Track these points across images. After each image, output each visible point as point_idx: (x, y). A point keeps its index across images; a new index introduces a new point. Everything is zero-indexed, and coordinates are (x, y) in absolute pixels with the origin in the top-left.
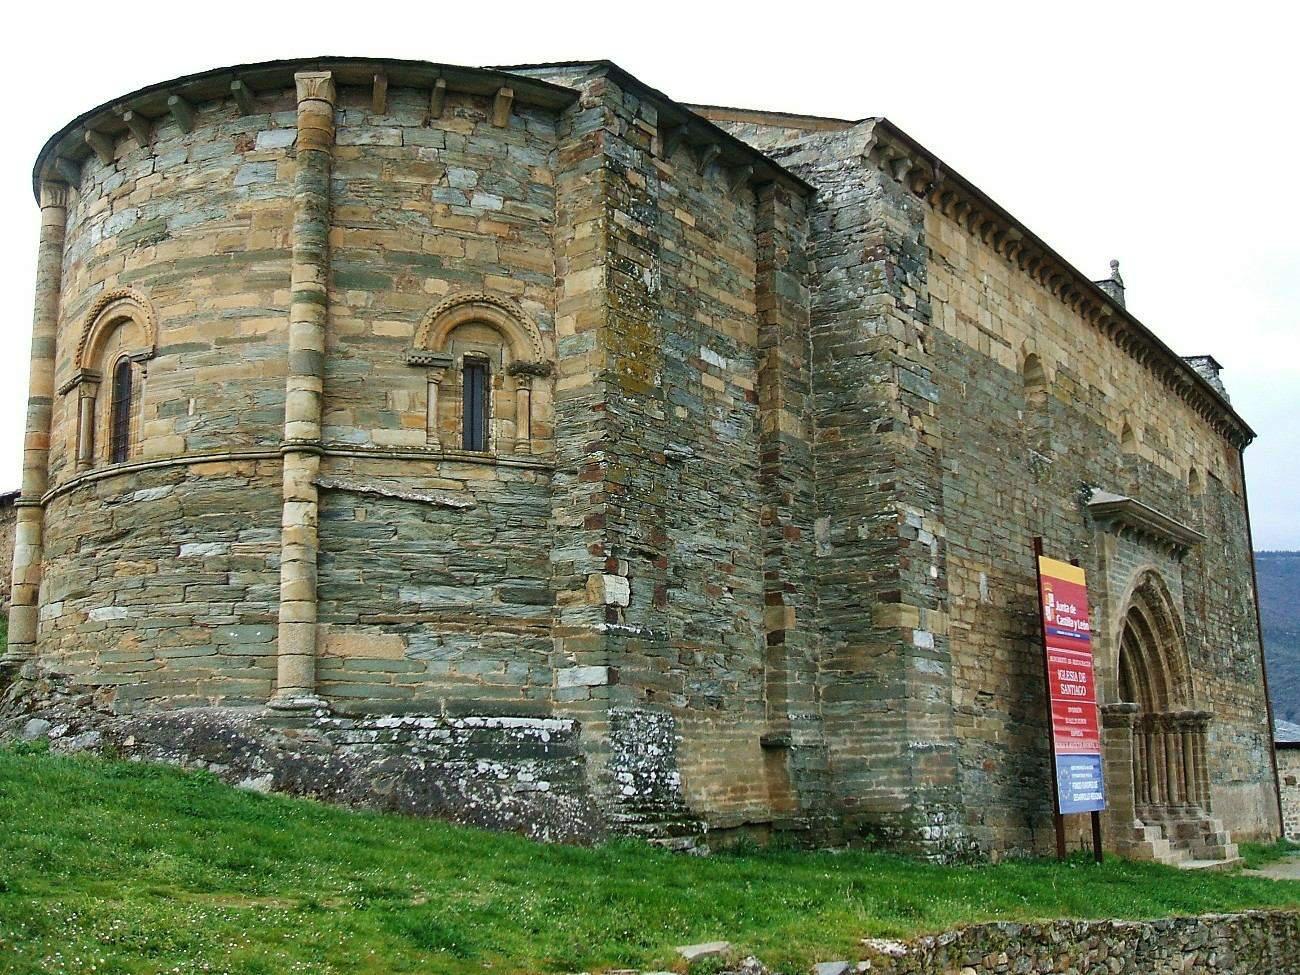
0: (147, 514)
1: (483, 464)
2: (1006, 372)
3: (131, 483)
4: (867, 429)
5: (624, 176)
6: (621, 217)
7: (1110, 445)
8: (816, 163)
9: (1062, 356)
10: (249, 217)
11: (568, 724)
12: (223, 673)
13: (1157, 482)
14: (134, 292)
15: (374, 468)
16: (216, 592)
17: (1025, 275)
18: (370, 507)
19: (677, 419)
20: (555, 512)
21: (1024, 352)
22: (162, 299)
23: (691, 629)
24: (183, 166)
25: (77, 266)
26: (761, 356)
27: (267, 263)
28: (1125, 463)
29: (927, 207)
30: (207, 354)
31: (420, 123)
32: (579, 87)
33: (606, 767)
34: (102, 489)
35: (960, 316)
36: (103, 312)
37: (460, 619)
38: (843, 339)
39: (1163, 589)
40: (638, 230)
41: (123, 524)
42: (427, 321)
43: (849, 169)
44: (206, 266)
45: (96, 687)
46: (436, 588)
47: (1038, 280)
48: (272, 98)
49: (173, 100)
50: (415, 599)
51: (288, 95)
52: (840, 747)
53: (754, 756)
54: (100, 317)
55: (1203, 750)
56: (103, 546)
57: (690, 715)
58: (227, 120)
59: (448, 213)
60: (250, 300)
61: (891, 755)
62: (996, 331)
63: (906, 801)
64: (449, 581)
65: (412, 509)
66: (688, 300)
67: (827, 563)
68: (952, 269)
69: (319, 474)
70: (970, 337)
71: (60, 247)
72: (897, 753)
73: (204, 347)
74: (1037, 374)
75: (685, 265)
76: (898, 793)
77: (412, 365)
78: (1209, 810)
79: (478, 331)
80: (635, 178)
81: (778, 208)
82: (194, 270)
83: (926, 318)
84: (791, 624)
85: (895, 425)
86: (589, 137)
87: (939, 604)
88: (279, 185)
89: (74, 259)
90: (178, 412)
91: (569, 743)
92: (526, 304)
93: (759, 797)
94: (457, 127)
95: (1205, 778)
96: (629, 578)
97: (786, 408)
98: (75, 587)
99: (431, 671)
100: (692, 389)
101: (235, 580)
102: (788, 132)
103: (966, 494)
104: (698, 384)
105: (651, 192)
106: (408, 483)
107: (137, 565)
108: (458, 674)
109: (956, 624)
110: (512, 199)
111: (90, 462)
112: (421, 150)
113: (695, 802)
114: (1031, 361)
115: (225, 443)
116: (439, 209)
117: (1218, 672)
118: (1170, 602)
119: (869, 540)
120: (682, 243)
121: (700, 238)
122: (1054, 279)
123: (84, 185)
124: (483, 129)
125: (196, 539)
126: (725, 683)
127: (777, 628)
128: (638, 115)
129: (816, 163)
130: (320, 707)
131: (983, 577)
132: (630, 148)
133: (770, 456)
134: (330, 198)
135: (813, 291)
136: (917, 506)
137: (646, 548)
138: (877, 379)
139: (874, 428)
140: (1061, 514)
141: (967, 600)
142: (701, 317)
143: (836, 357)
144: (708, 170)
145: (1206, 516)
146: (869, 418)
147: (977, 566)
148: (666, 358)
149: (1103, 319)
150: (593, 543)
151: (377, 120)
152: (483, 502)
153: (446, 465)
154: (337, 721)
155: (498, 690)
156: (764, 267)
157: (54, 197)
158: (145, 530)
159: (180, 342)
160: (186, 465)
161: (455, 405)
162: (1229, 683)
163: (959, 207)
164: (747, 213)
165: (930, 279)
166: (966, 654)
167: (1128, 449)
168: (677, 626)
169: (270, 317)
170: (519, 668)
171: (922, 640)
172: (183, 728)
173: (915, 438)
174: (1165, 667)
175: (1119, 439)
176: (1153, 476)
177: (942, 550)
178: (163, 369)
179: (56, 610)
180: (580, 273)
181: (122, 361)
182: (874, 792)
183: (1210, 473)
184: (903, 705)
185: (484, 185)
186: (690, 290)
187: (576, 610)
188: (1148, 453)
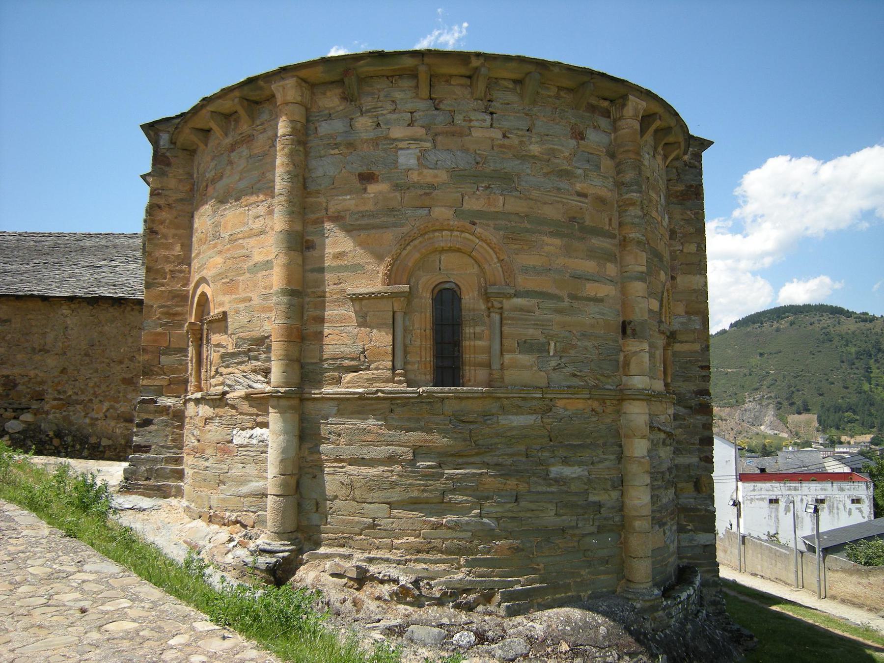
10: (585, 196)
22: (516, 246)
24: (527, 133)
33: (715, 596)
44: (557, 230)
60: (589, 266)
73: (559, 299)
88: (604, 177)
90: (540, 351)
125: (565, 461)
150: (705, 454)
158: (509, 451)
159: (537, 289)
169: (605, 284)
178: (522, 310)
180: (689, 276)
181: (447, 286)
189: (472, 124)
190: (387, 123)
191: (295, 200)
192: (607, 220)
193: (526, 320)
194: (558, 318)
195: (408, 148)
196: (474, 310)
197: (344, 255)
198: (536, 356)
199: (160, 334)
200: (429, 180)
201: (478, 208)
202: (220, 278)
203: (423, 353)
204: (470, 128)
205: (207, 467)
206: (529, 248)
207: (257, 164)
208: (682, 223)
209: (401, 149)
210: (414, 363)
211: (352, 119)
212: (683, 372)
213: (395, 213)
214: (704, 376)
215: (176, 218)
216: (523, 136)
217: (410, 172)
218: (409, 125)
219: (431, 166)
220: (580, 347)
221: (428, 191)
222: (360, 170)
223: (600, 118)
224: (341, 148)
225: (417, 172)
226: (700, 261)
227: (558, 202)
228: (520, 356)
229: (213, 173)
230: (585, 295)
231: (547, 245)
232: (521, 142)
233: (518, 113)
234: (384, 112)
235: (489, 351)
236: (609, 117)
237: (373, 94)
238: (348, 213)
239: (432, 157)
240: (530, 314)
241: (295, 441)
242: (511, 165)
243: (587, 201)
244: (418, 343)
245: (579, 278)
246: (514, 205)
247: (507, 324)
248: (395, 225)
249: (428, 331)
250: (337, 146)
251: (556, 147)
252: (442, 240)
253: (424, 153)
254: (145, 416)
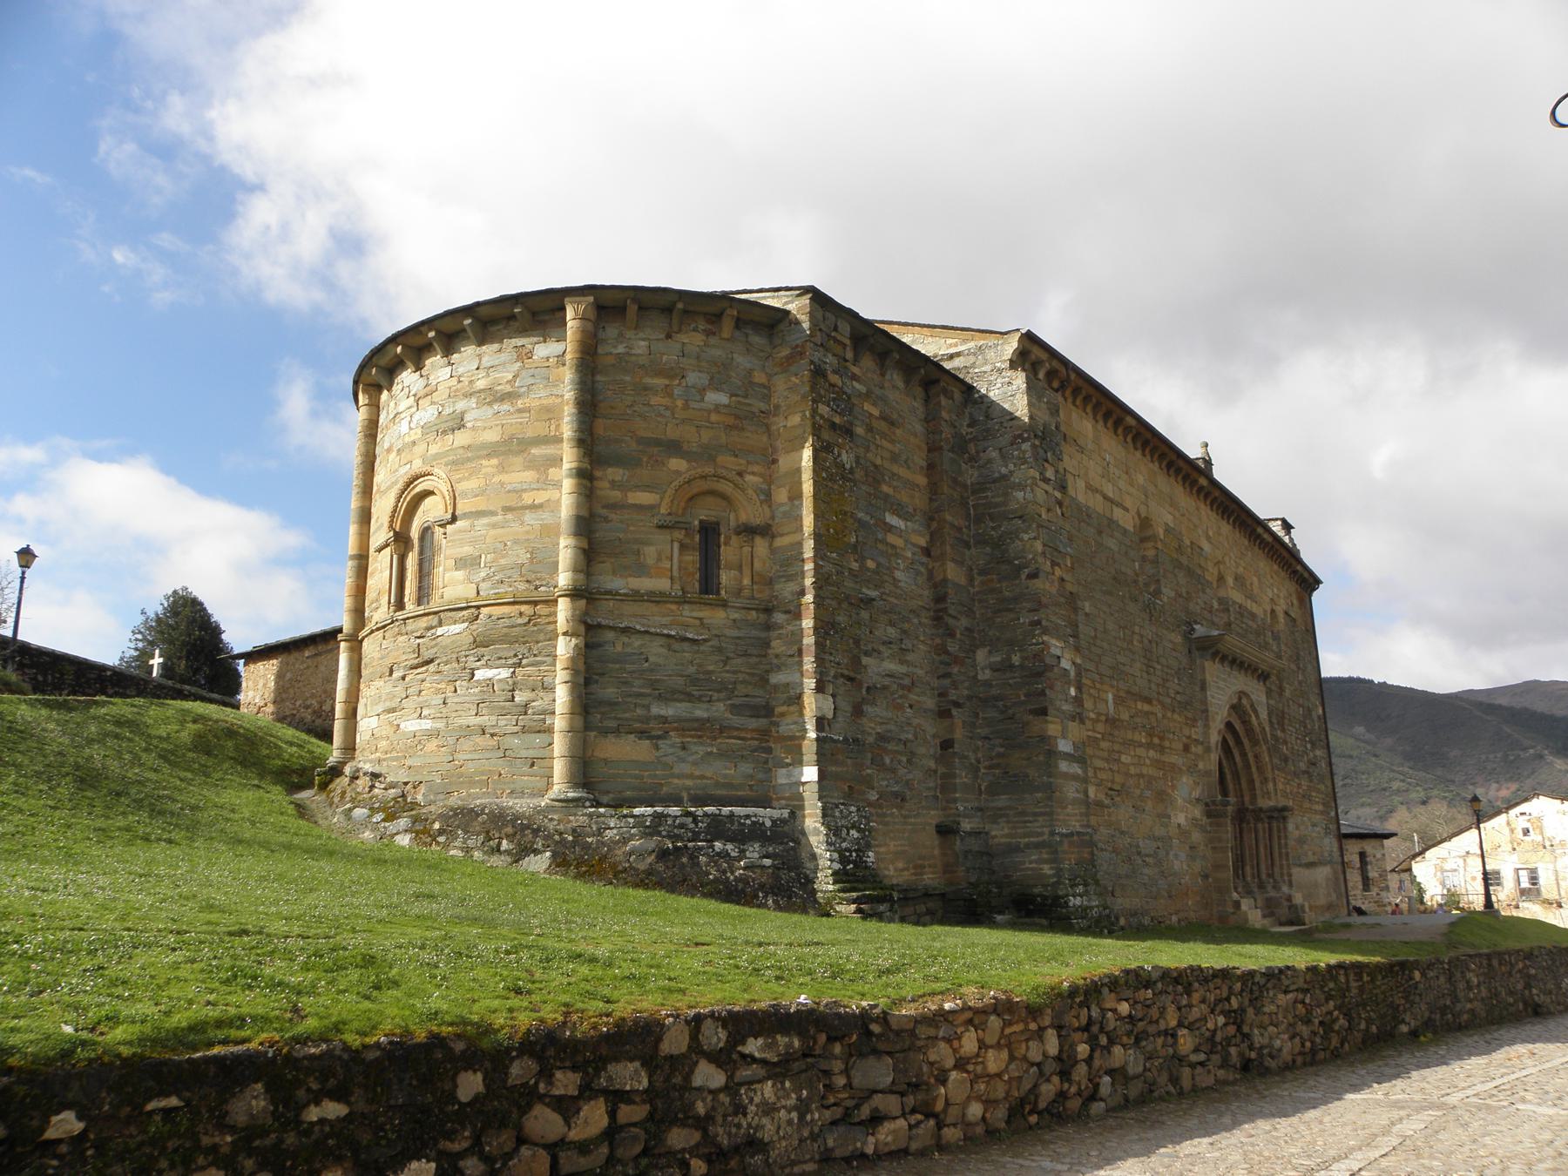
0: (447, 646)
1: (717, 605)
2: (1125, 531)
3: (434, 620)
4: (1018, 576)
5: (825, 376)
6: (823, 409)
7: (1208, 590)
8: (973, 365)
9: (1169, 519)
11: (786, 813)
13: (1245, 620)
14: (436, 471)
15: (629, 608)
16: (503, 708)
17: (1138, 454)
18: (626, 640)
19: (868, 569)
20: (774, 644)
21: (1139, 515)
23: (882, 738)
25: (389, 450)
26: (931, 519)
28: (1220, 604)
29: (1061, 399)
30: (494, 519)
31: (662, 336)
32: (789, 307)
34: (411, 625)
35: (1089, 487)
37: (701, 728)
38: (997, 505)
39: (1252, 706)
40: (837, 420)
41: (427, 655)
42: (670, 492)
43: (1000, 371)
45: (406, 784)
46: (678, 705)
47: (1149, 457)
48: (547, 318)
49: (468, 322)
50: (663, 712)
51: (558, 315)
52: (1000, 833)
53: (930, 841)
55: (1286, 837)
57: (881, 807)
59: (686, 407)
61: (1040, 839)
62: (1117, 499)
63: (1054, 876)
64: (689, 697)
65: (662, 641)
66: (875, 476)
67: (987, 684)
68: (1082, 450)
69: (586, 613)
70: (1096, 503)
71: (375, 436)
72: (1046, 837)
74: (1150, 533)
75: (872, 447)
76: (1047, 869)
77: (660, 527)
78: (1291, 885)
79: (710, 500)
80: (834, 379)
81: (944, 401)
83: (1063, 488)
84: (959, 734)
85: (1041, 574)
86: (797, 346)
87: (1079, 717)
89: (386, 445)
90: (472, 565)
91: (786, 828)
92: (749, 478)
93: (933, 873)
94: (692, 339)
95: (1287, 860)
96: (833, 696)
97: (953, 560)
98: (388, 704)
99: (676, 771)
100: (880, 546)
101: (520, 697)
102: (950, 341)
103: (1096, 630)
104: (883, 541)
105: (846, 389)
106: (657, 619)
108: (697, 773)
109: (1090, 733)
110: (737, 395)
111: (400, 605)
112: (665, 358)
113: (885, 876)
114: (1145, 522)
116: (679, 403)
117: (1295, 774)
118: (1257, 717)
119: (1022, 666)
120: (870, 429)
121: (883, 425)
122: (1162, 456)
123: (394, 388)
124: (713, 340)
125: (487, 666)
126: (907, 782)
127: (949, 737)
128: (836, 329)
129: (973, 365)
130: (588, 799)
131: (1110, 696)
132: (830, 355)
133: (940, 599)
134: (593, 396)
135: (972, 467)
136: (1058, 638)
137: (846, 672)
138: (1026, 537)
139: (1023, 577)
140: (1170, 646)
141: (1099, 714)
142: (885, 488)
143: (992, 519)
144: (889, 372)
145: (1283, 647)
146: (1020, 568)
147: (1106, 687)
148: (859, 521)
149: (1201, 489)
151: (629, 334)
152: (716, 636)
153: (686, 607)
154: (602, 810)
155: (729, 786)
156: (933, 448)
157: (370, 398)
160: (478, 607)
161: (693, 558)
162: (1305, 783)
163: (1087, 399)
164: (918, 405)
165: (1066, 458)
166: (1099, 757)
167: (1222, 593)
168: (869, 734)
170: (746, 768)
171: (1064, 746)
172: (478, 815)
173: (1056, 584)
174: (1254, 769)
175: (1215, 585)
176: (1242, 616)
177: (1079, 674)
178: (460, 531)
179: (374, 722)
182: (1028, 869)
183: (1286, 613)
184: (1050, 798)
185: (715, 385)
186: (876, 466)
188: (1237, 596)
194: (492, 532)
252: (421, 486)
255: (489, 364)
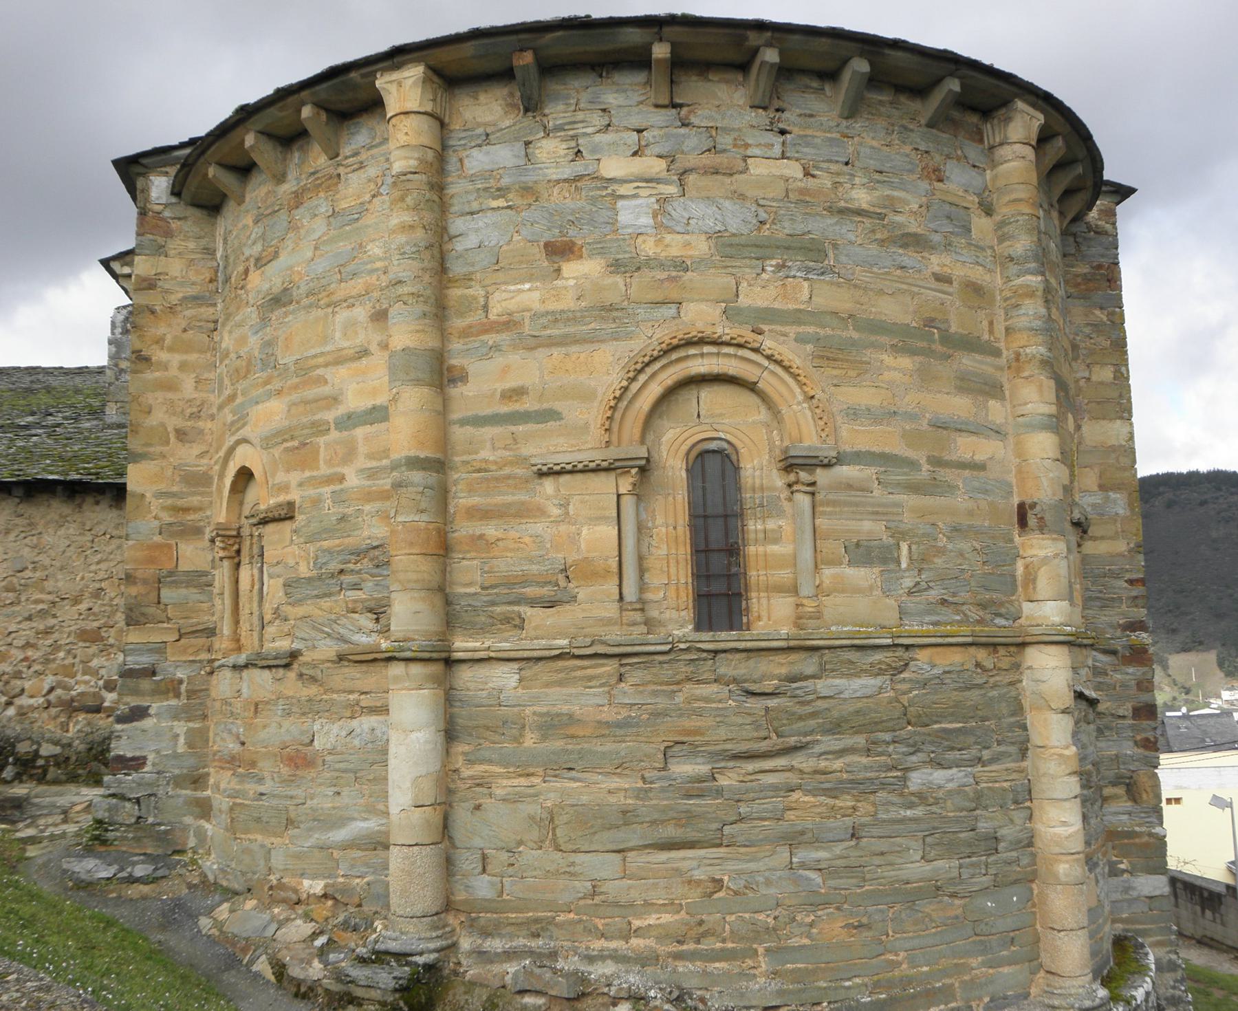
3: (809, 665)
10: (949, 281)
12: (983, 964)
22: (835, 372)
27: (978, 357)
33: (1174, 988)
36: (674, 356)
54: (664, 361)
56: (731, 764)
58: (904, 122)
60: (959, 406)
73: (913, 464)
82: (885, 339)
90: (884, 561)
98: (670, 832)
107: (839, 803)
115: (958, 618)
150: (1144, 735)
159: (875, 449)
169: (987, 437)
178: (850, 487)
181: (713, 446)
187: (1121, 810)
189: (749, 152)
190: (595, 149)
191: (428, 292)
192: (985, 323)
193: (857, 505)
194: (911, 500)
195: (635, 196)
196: (762, 488)
197: (522, 394)
198: (876, 570)
199: (159, 546)
200: (675, 252)
201: (765, 304)
202: (279, 440)
203: (673, 570)
204: (745, 158)
205: (262, 794)
206: (859, 375)
207: (347, 228)
208: (1087, 330)
209: (622, 197)
210: (658, 589)
211: (527, 144)
212: (1101, 592)
213: (615, 314)
214: (1136, 597)
215: (185, 330)
216: (838, 174)
217: (640, 239)
218: (635, 154)
219: (678, 229)
220: (951, 551)
221: (674, 274)
222: (547, 237)
223: (967, 142)
224: (511, 196)
225: (653, 239)
226: (1121, 396)
227: (904, 292)
228: (850, 571)
229: (258, 248)
230: (954, 458)
231: (889, 368)
232: (836, 185)
233: (829, 132)
234: (589, 130)
235: (794, 561)
236: (981, 141)
237: (568, 97)
238: (527, 314)
239: (678, 210)
240: (865, 494)
241: (440, 738)
242: (822, 226)
243: (951, 290)
244: (663, 551)
245: (945, 428)
246: (830, 297)
247: (824, 513)
248: (615, 337)
249: (680, 529)
250: (502, 192)
251: (896, 194)
253: (663, 200)
254: (134, 701)
255: (873, 164)
